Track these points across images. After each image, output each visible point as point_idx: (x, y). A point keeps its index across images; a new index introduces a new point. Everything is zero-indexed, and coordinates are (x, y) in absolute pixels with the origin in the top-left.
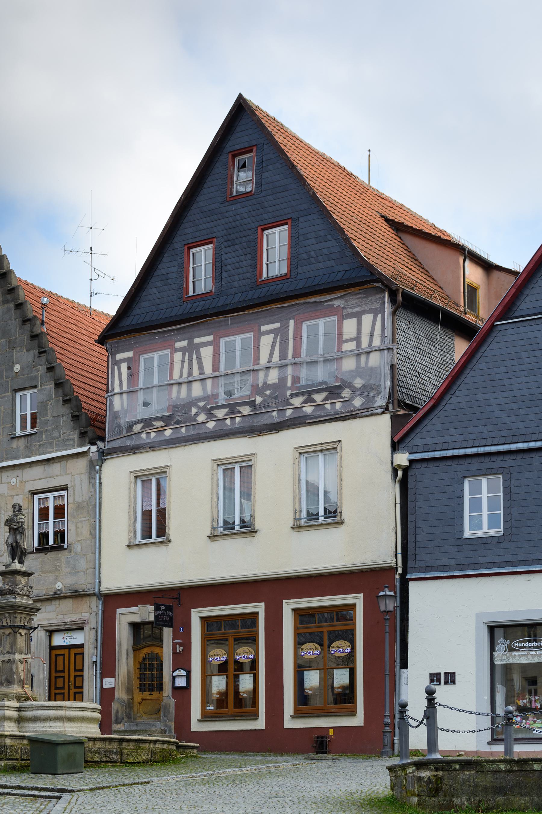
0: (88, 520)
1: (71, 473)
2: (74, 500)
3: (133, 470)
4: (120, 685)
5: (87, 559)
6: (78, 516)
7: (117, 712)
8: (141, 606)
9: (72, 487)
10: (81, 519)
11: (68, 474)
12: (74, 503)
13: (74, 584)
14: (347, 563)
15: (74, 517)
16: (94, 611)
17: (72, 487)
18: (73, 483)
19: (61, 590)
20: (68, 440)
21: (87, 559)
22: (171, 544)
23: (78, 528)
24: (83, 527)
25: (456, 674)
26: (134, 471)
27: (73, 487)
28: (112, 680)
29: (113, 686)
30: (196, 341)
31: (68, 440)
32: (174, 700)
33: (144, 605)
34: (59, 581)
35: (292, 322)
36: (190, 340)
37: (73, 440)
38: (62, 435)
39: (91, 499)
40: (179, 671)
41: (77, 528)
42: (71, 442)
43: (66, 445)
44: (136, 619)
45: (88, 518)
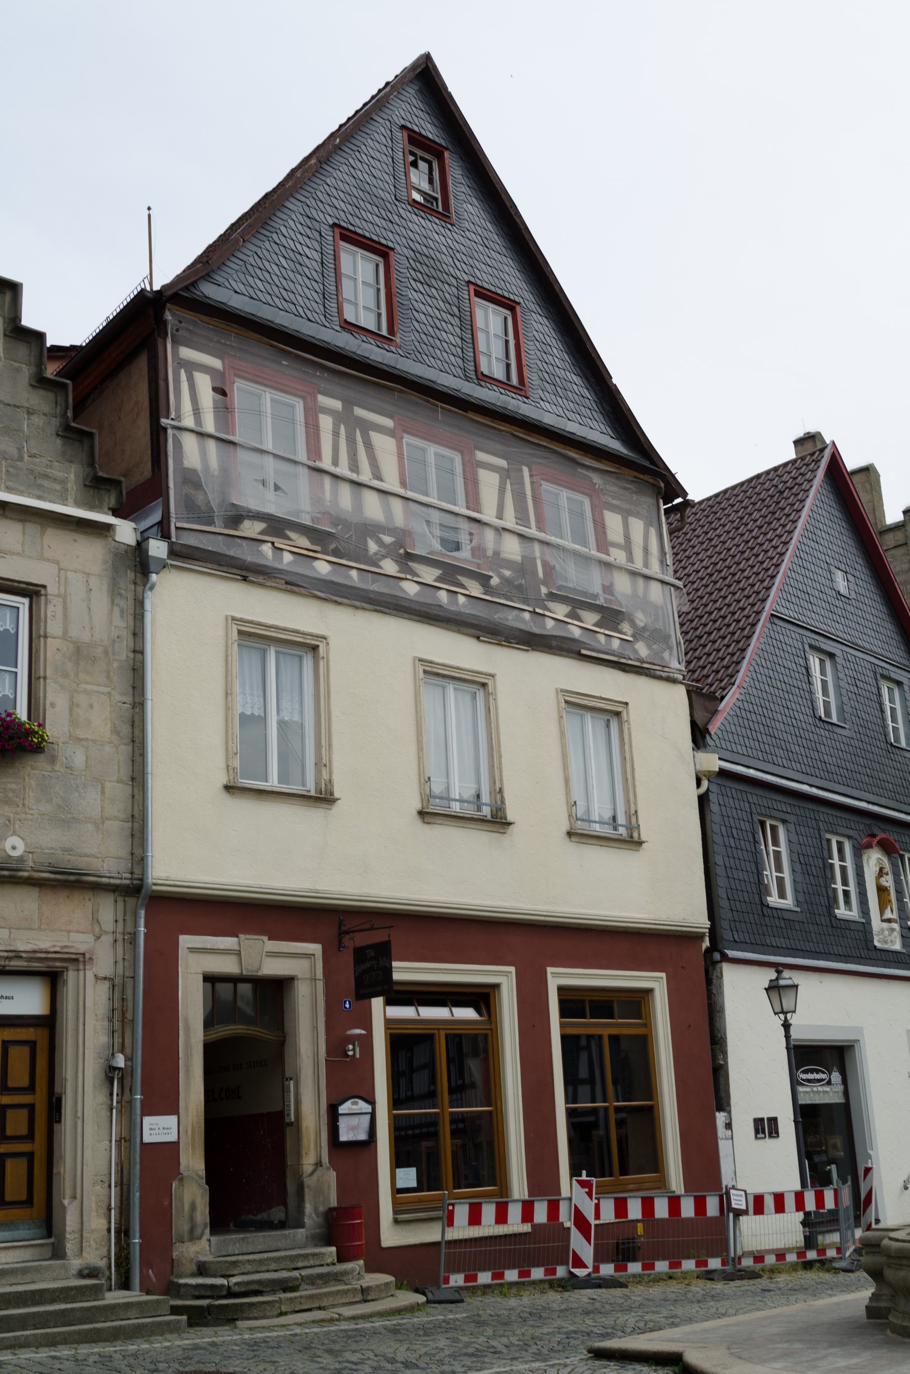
0: (109, 693)
1: (58, 563)
2: (65, 632)
3: (238, 615)
4: (190, 1133)
5: (103, 792)
6: (77, 674)
7: (193, 1207)
8: (248, 936)
9: (58, 596)
10: (83, 686)
11: (48, 560)
12: (65, 636)
13: (64, 850)
14: (652, 916)
15: (65, 675)
16: (106, 933)
17: (58, 596)
18: (62, 589)
19: (21, 859)
20: (46, 476)
21: (103, 792)
22: (337, 808)
23: (78, 706)
24: (91, 706)
25: (779, 1120)
26: (241, 620)
27: (64, 598)
28: (170, 1121)
29: (173, 1138)
30: (359, 412)
31: (46, 476)
32: (335, 1173)
33: (256, 937)
34: (14, 833)
35: (525, 470)
36: (349, 404)
37: (63, 482)
38: (26, 457)
39: (117, 645)
40: (353, 1104)
41: (73, 706)
42: (58, 487)
43: (40, 487)
44: (227, 966)
45: (107, 690)
